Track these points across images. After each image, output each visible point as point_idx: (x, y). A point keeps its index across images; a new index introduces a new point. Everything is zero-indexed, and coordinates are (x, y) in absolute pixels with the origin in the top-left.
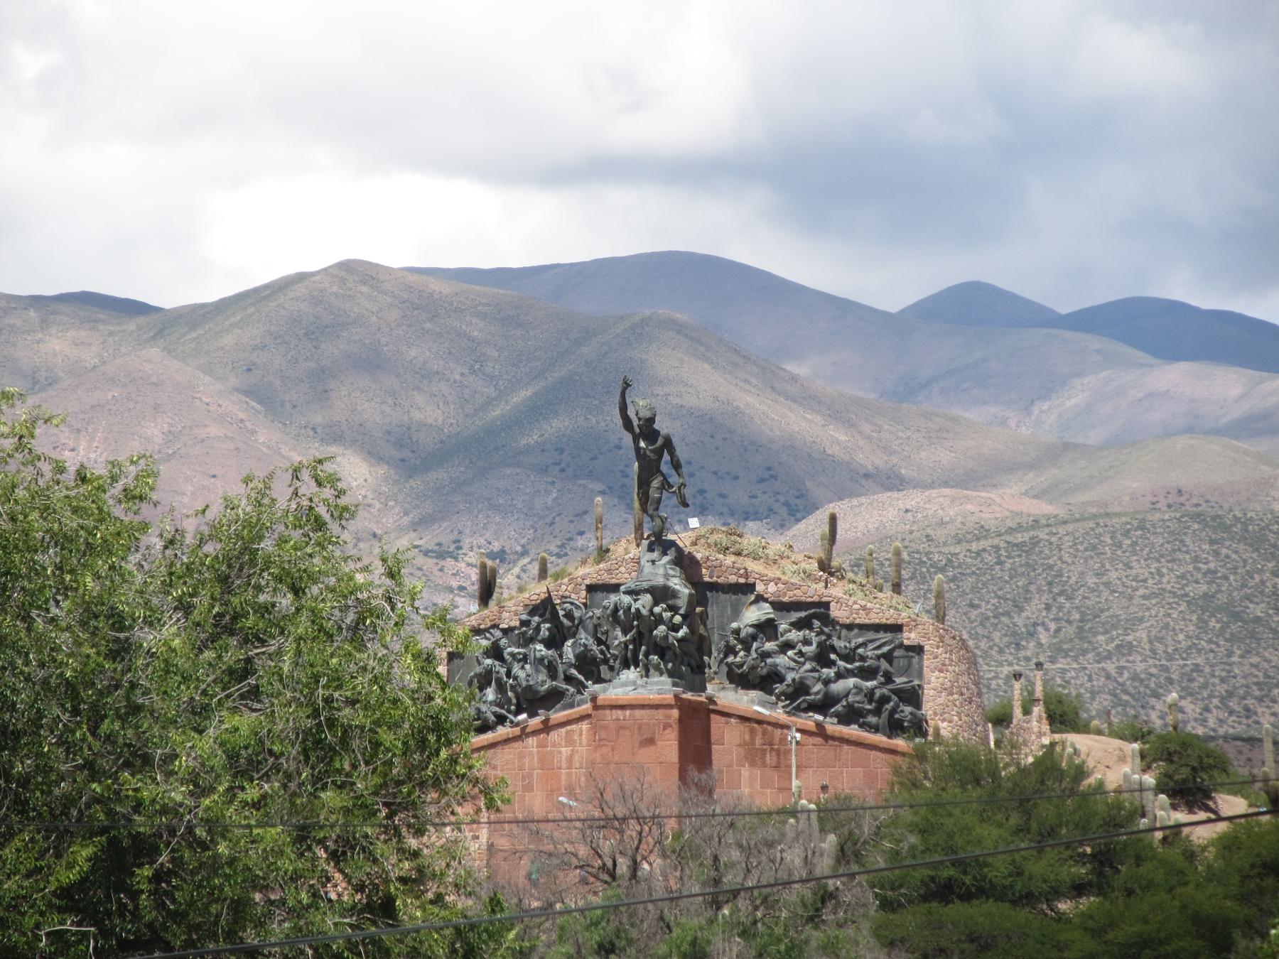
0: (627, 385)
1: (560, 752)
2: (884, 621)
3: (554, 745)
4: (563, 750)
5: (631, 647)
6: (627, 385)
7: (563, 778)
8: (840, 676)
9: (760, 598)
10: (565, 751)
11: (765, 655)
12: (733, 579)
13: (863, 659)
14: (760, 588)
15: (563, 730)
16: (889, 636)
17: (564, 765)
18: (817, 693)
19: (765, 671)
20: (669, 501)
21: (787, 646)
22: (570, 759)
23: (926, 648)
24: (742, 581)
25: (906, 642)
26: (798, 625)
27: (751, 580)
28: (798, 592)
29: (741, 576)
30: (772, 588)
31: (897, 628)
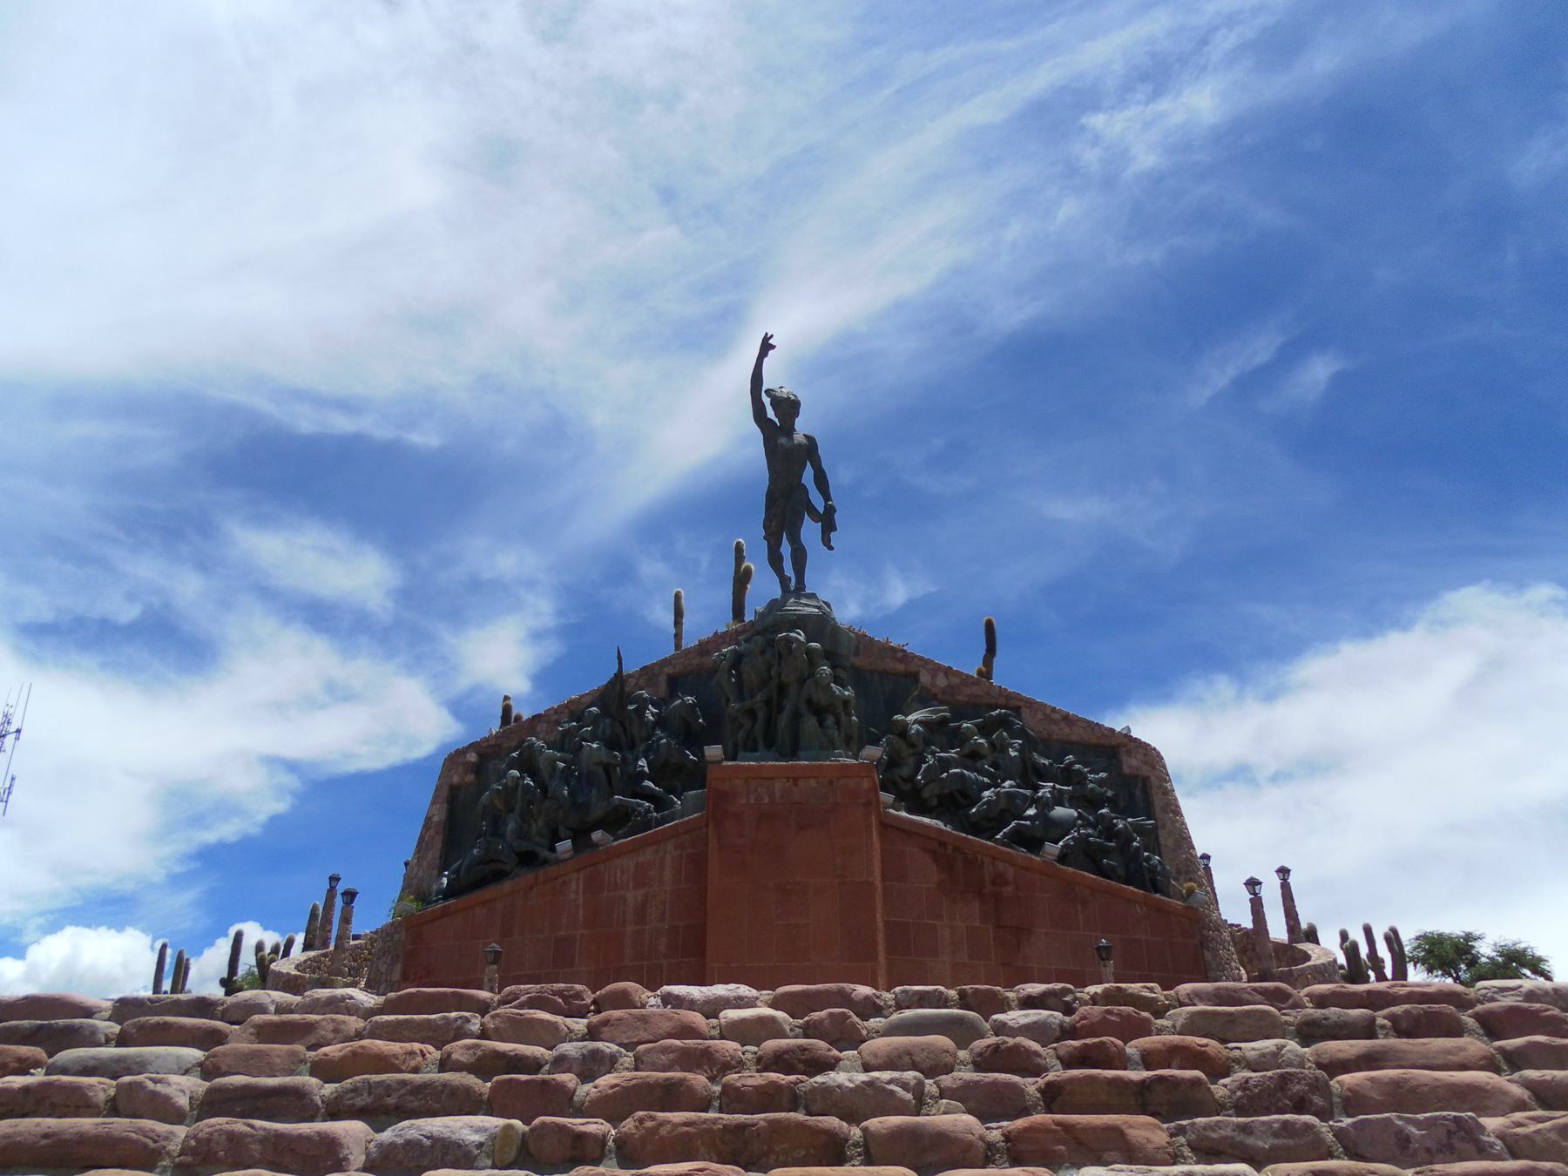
0: (766, 346)
2: (1094, 741)
5: (761, 715)
6: (766, 346)
8: (1058, 799)
10: (633, 896)
11: (945, 764)
14: (925, 678)
18: (1029, 818)
21: (973, 757)
23: (1153, 779)
24: (901, 667)
25: (1126, 770)
27: (913, 668)
29: (901, 661)
30: (941, 681)
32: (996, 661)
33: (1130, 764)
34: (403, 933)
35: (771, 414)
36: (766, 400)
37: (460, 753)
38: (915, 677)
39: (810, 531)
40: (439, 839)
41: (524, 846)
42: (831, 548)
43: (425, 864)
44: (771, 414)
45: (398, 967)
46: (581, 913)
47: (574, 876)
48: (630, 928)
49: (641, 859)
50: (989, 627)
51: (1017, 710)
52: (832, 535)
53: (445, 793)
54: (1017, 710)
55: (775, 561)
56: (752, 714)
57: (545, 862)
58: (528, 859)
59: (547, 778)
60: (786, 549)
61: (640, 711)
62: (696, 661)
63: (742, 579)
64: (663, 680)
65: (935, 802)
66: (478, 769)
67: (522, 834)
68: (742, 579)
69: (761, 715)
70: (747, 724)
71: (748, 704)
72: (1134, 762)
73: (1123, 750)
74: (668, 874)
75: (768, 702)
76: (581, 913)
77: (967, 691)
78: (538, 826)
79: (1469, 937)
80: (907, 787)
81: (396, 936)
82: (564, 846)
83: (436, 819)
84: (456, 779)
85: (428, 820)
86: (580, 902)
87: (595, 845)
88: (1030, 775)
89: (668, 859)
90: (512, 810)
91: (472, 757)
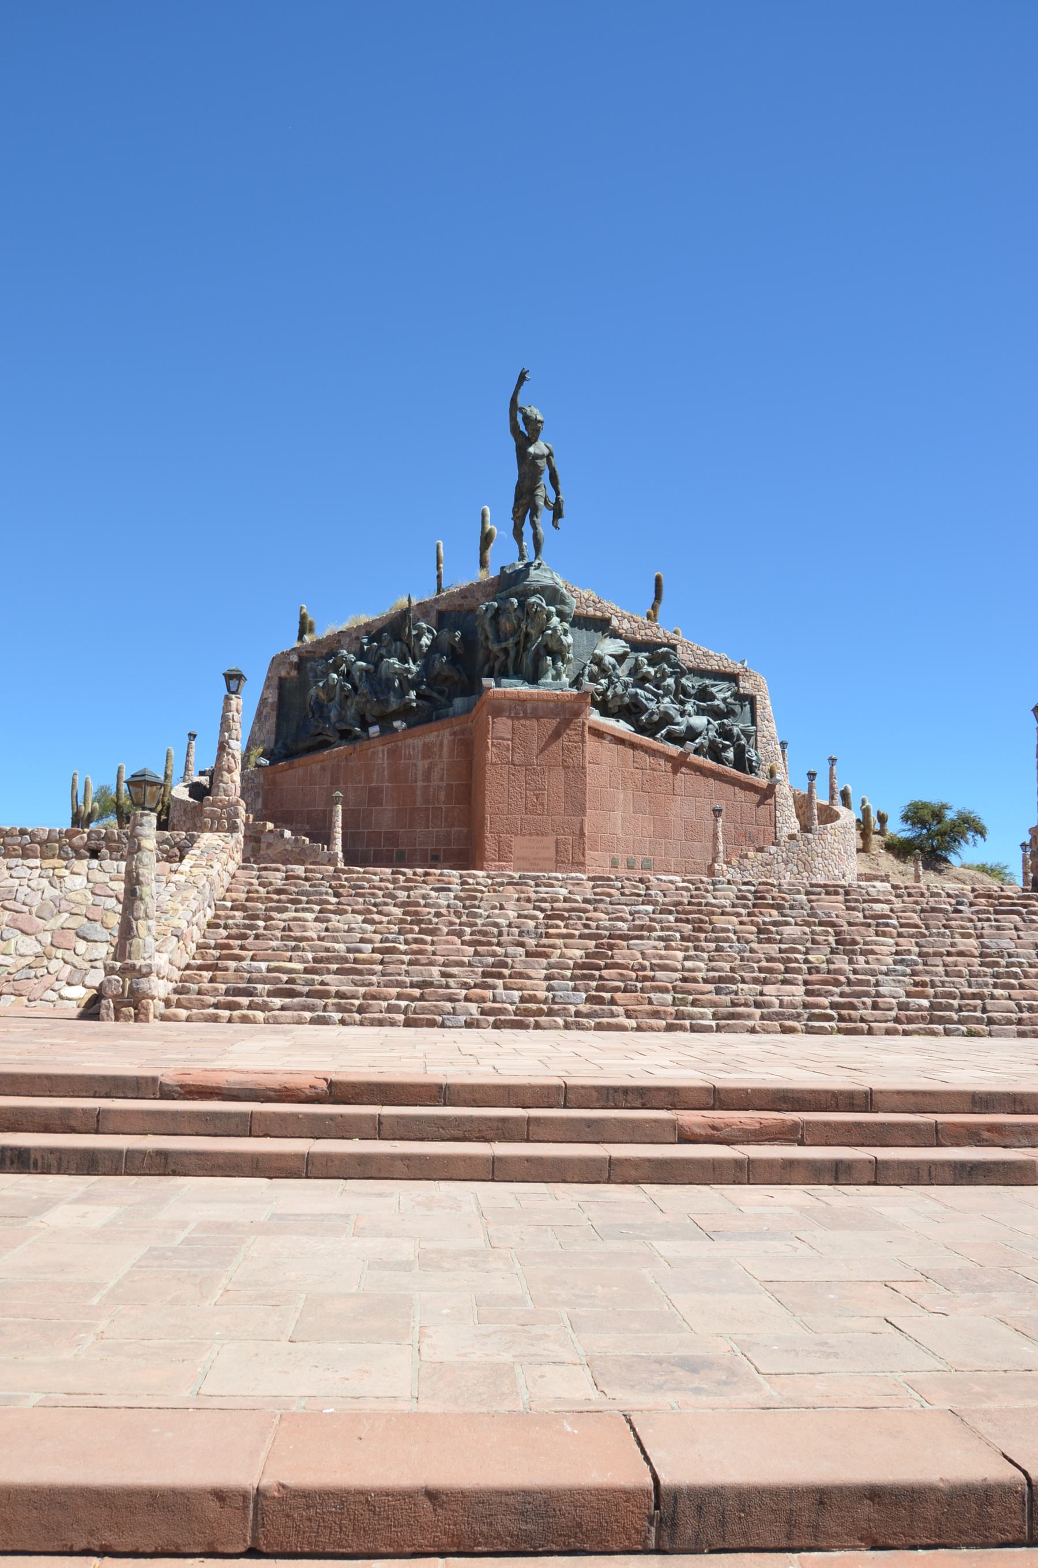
0: (522, 378)
1: (415, 765)
3: (410, 757)
4: (420, 764)
5: (512, 653)
6: (522, 378)
7: (419, 792)
9: (615, 635)
10: (422, 765)
11: (626, 686)
12: (591, 611)
13: (713, 697)
14: (615, 622)
15: (419, 742)
16: (725, 685)
17: (420, 777)
18: (678, 724)
19: (627, 700)
20: (545, 516)
22: (427, 776)
23: (758, 698)
24: (599, 614)
26: (652, 663)
27: (608, 615)
28: (648, 632)
30: (626, 625)
31: (733, 678)
32: (661, 608)
33: (746, 686)
34: (262, 779)
35: (522, 428)
36: (519, 417)
37: (286, 655)
38: (608, 621)
39: (545, 516)
40: (274, 713)
41: (344, 727)
42: (556, 527)
43: (265, 731)
44: (522, 428)
45: (260, 800)
46: (386, 773)
47: (380, 748)
48: (420, 784)
49: (427, 740)
50: (658, 580)
51: (674, 647)
52: (560, 520)
53: (275, 682)
54: (674, 647)
55: (518, 535)
56: (506, 650)
57: (357, 738)
58: (346, 735)
59: (357, 681)
60: (527, 529)
61: (419, 637)
62: (458, 601)
63: (486, 539)
64: (433, 615)
65: (616, 710)
66: (299, 666)
67: (341, 719)
68: (486, 539)
69: (512, 653)
70: (502, 657)
71: (504, 645)
72: (747, 685)
73: (741, 678)
74: (445, 749)
75: (517, 644)
76: (386, 773)
77: (643, 632)
78: (351, 712)
79: (944, 807)
80: (599, 698)
81: (256, 781)
82: (374, 730)
83: (270, 700)
84: (283, 674)
85: (263, 702)
86: (385, 765)
87: (396, 730)
88: (681, 694)
89: (445, 742)
90: (331, 700)
91: (295, 659)
